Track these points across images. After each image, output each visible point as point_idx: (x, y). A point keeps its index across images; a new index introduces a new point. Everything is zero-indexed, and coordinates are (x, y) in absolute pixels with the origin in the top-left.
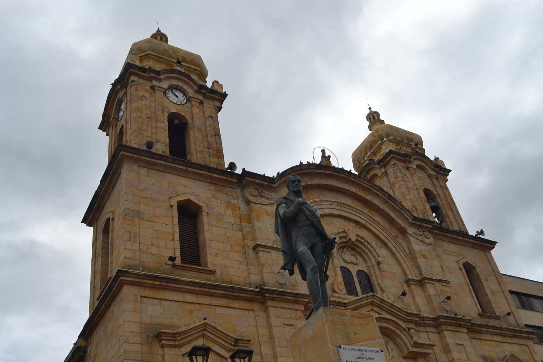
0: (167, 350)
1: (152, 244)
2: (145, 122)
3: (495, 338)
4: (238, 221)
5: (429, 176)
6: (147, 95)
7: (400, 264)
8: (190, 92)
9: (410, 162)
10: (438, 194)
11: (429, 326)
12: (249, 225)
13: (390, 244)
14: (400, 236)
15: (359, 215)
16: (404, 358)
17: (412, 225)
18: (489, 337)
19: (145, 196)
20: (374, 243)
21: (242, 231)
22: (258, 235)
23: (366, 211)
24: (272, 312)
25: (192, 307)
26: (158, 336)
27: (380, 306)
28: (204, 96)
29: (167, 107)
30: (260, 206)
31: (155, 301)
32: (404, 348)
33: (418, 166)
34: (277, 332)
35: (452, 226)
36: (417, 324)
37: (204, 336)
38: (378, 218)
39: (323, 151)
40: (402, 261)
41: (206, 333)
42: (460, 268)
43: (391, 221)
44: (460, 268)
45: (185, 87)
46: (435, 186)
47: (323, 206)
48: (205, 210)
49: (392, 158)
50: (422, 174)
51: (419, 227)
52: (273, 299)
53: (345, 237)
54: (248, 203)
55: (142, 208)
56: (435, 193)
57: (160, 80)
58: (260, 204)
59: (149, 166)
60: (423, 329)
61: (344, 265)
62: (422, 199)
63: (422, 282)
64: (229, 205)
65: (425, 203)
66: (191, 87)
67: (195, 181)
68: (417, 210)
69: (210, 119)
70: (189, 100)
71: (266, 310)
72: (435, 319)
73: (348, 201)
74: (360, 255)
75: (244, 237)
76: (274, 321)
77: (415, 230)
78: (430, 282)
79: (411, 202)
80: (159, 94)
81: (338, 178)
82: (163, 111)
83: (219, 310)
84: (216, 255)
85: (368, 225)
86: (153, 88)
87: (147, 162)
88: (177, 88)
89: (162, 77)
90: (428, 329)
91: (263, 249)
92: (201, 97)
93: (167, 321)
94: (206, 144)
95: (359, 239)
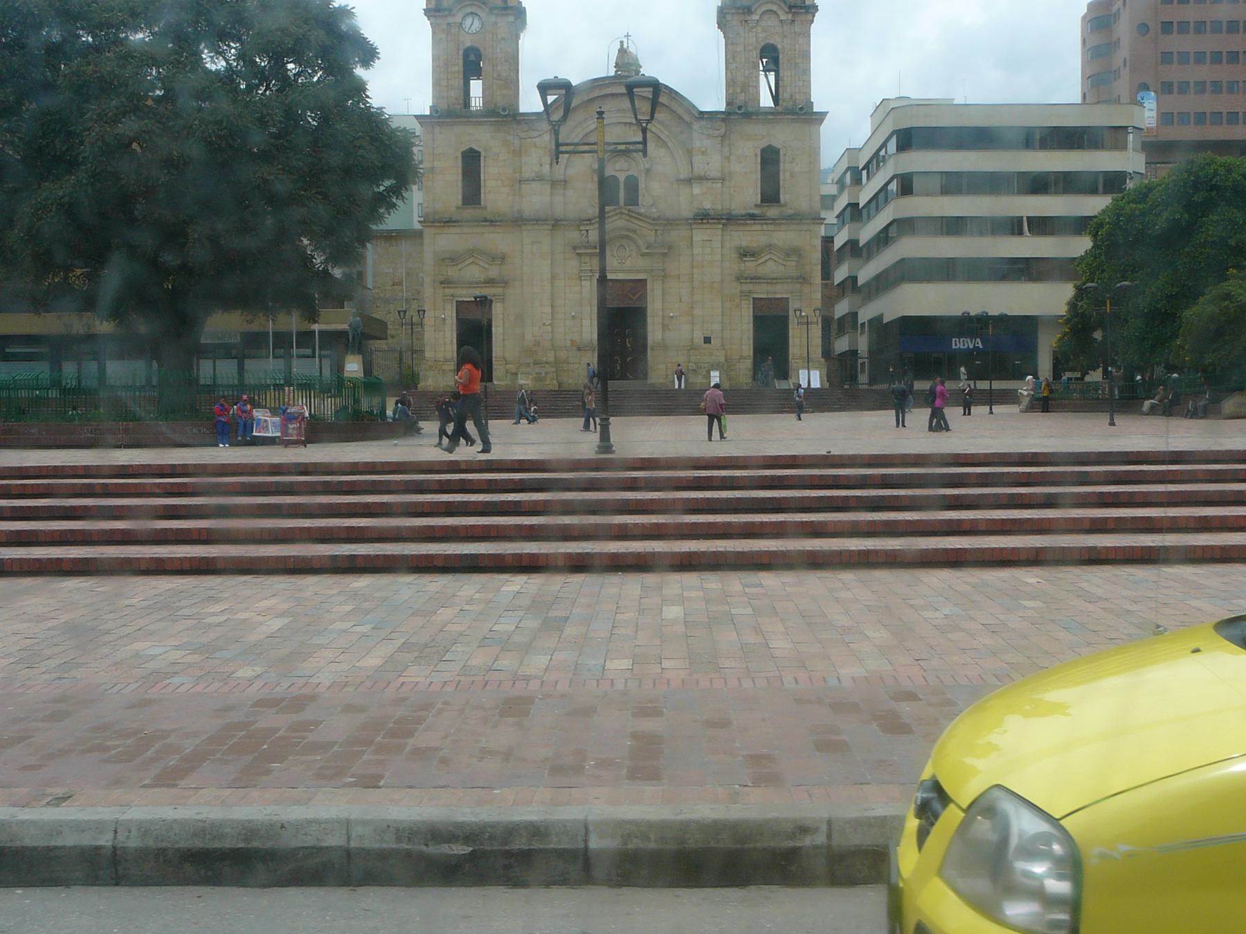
3: (765, 227)
13: (670, 144)
30: (530, 140)
37: (473, 256)
48: (483, 154)
50: (770, 22)
57: (454, 15)
58: (530, 138)
74: (635, 161)
94: (495, 75)
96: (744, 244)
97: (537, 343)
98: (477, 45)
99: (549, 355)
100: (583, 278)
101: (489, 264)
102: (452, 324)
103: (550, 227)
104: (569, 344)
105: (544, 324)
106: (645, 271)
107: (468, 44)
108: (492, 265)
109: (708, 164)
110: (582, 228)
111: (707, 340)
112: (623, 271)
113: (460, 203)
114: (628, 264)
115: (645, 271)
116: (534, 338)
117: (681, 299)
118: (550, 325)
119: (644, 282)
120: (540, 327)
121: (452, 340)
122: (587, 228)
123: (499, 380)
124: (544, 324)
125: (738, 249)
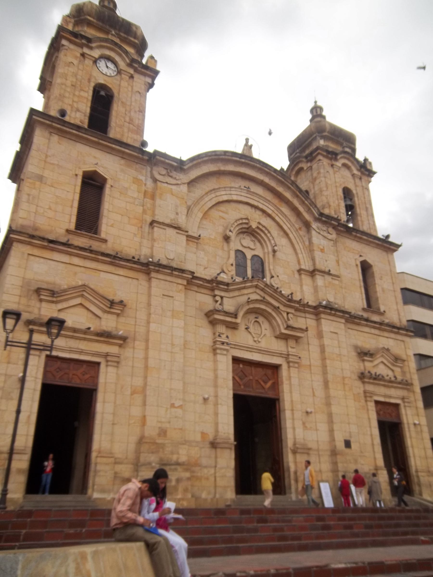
0: (44, 304)
1: (50, 209)
2: (68, 89)
3: (373, 331)
4: (141, 196)
5: (353, 175)
6: (75, 62)
7: (296, 254)
8: (122, 65)
9: (336, 160)
10: (357, 194)
11: (309, 313)
12: (151, 202)
13: (291, 235)
14: (304, 229)
15: (267, 205)
16: (277, 337)
17: (317, 220)
18: (367, 329)
19: (52, 162)
20: (275, 231)
21: (143, 206)
22: (157, 212)
23: (276, 201)
24: (154, 282)
25: (78, 269)
26: (38, 291)
27: (264, 290)
28: (136, 70)
29: (95, 77)
30: (166, 185)
31: (42, 260)
32: (278, 329)
33: (344, 165)
34: (154, 302)
35: (362, 225)
36: (297, 310)
37: (82, 296)
38: (285, 210)
39: (247, 140)
40: (299, 251)
41: (85, 293)
42: (357, 265)
43: (298, 214)
44: (357, 265)
45: (117, 58)
46: (356, 186)
47: (233, 192)
49: (319, 154)
50: (346, 173)
51: (324, 223)
52: (158, 271)
53: (247, 224)
54: (155, 180)
55: (46, 174)
56: (354, 192)
57: (91, 48)
58: (167, 183)
59: (62, 133)
60: (303, 315)
61: (241, 248)
62: (339, 197)
63: (313, 273)
64: (136, 181)
65: (340, 201)
66: (123, 59)
67: (106, 154)
68: (330, 206)
69: (138, 94)
70: (119, 72)
71: (150, 280)
72: (315, 308)
73: (259, 190)
74: (259, 241)
75: (144, 212)
76: (154, 290)
77: (319, 225)
78: (320, 274)
79: (327, 198)
80: (88, 62)
81: (253, 167)
82: (89, 80)
83: (103, 275)
84: (112, 226)
85: (274, 215)
86: (83, 55)
87: (59, 129)
88: (109, 59)
89: (94, 45)
90: (308, 315)
91: (158, 225)
92: (132, 71)
93: (50, 279)
94: (127, 119)
95: (261, 227)
96: (360, 344)
97: (163, 432)
98: (110, 86)
99: (181, 452)
100: (218, 351)
101: (105, 312)
102: (35, 390)
103: (185, 282)
104: (198, 438)
105: (173, 406)
106: (280, 355)
107: (102, 81)
108: (109, 312)
109: (326, 261)
110: (217, 292)
111: (348, 444)
112: (260, 351)
113: (72, 227)
114: (263, 344)
115: (280, 355)
116: (159, 425)
117: (313, 393)
118: (180, 407)
119: (276, 368)
120: (167, 409)
121: (29, 417)
122: (223, 294)
123: (103, 491)
124: (173, 406)
125: (356, 347)
